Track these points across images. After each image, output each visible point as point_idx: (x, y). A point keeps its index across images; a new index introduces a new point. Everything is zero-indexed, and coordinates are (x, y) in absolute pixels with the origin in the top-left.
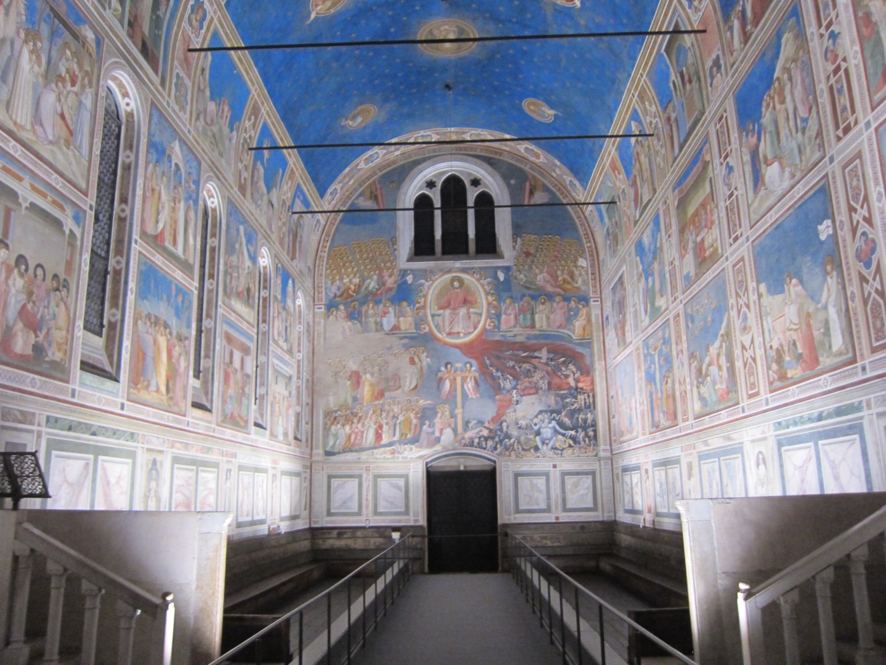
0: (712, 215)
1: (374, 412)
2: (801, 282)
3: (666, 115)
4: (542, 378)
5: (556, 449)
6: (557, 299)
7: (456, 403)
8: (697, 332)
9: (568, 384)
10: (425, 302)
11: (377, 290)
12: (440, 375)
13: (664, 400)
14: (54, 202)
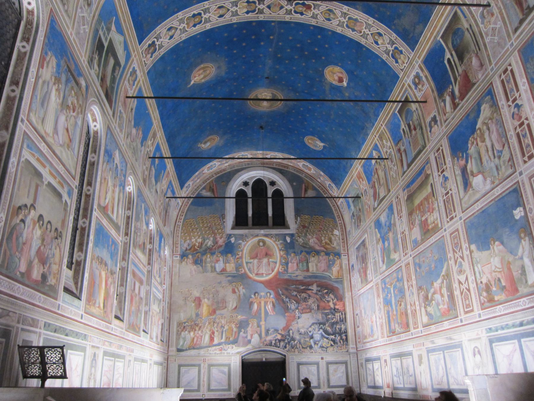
0: (433, 205)
1: (209, 323)
2: (502, 243)
3: (398, 148)
4: (313, 302)
5: (323, 347)
6: (322, 254)
7: (261, 318)
8: (423, 274)
9: (329, 306)
10: (242, 254)
11: (213, 246)
12: (251, 300)
13: (399, 316)
14: (59, 182)
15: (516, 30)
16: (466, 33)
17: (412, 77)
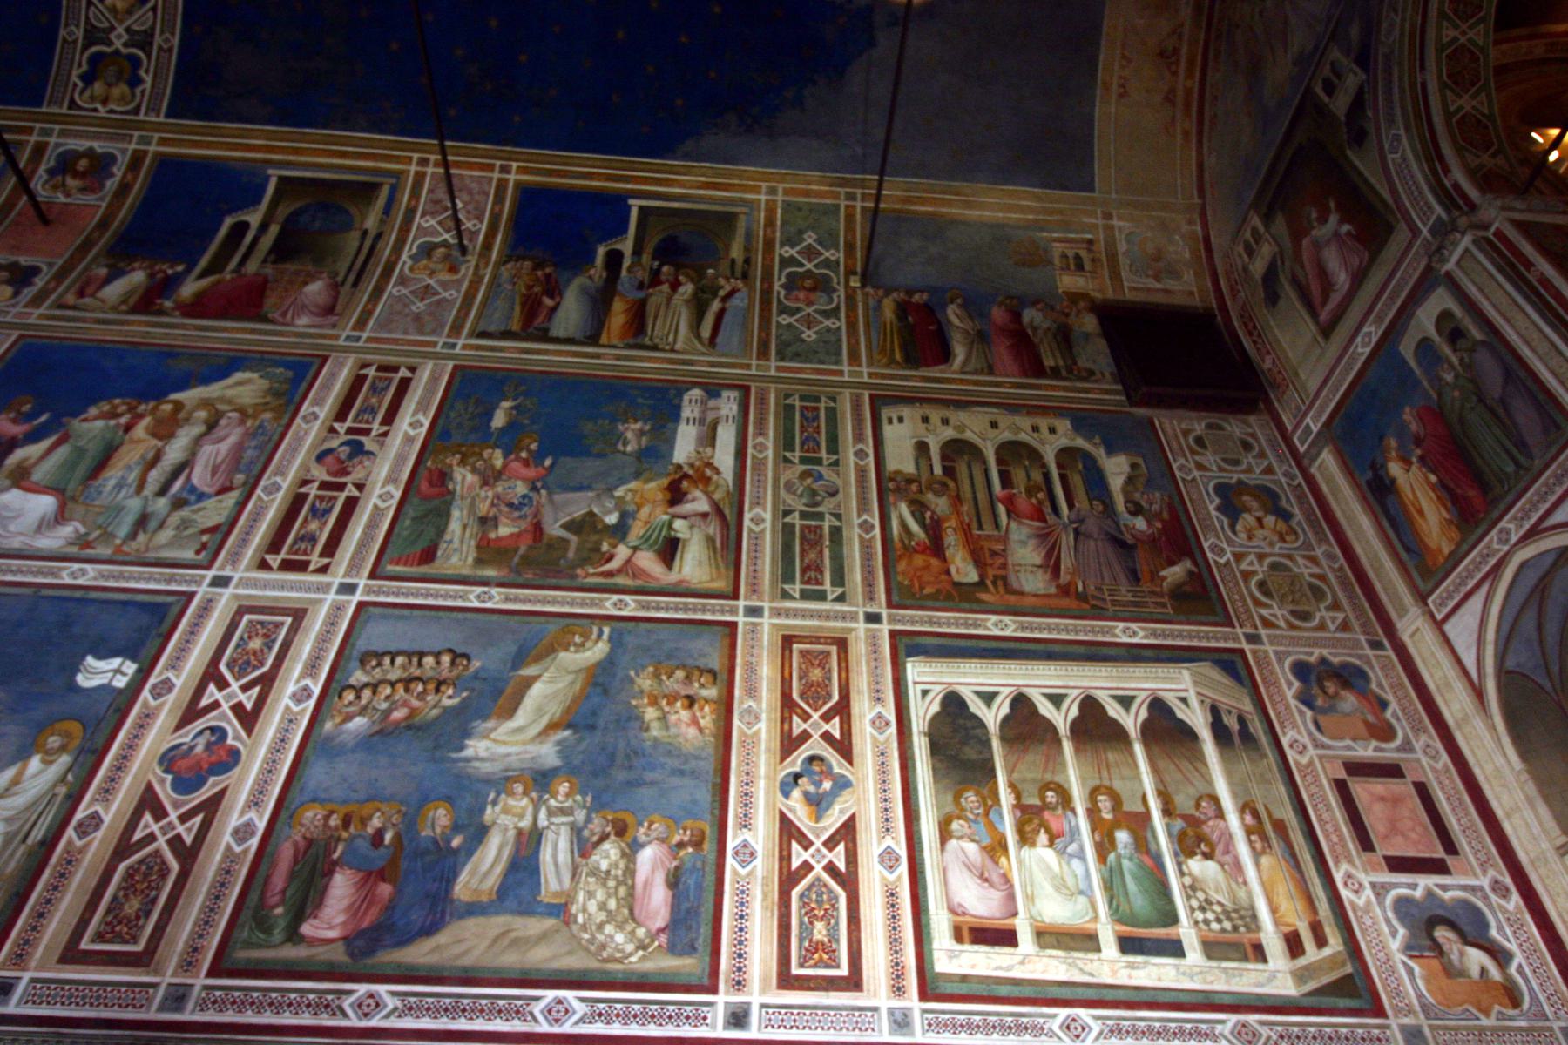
15: (483, 335)
17: (82, 144)
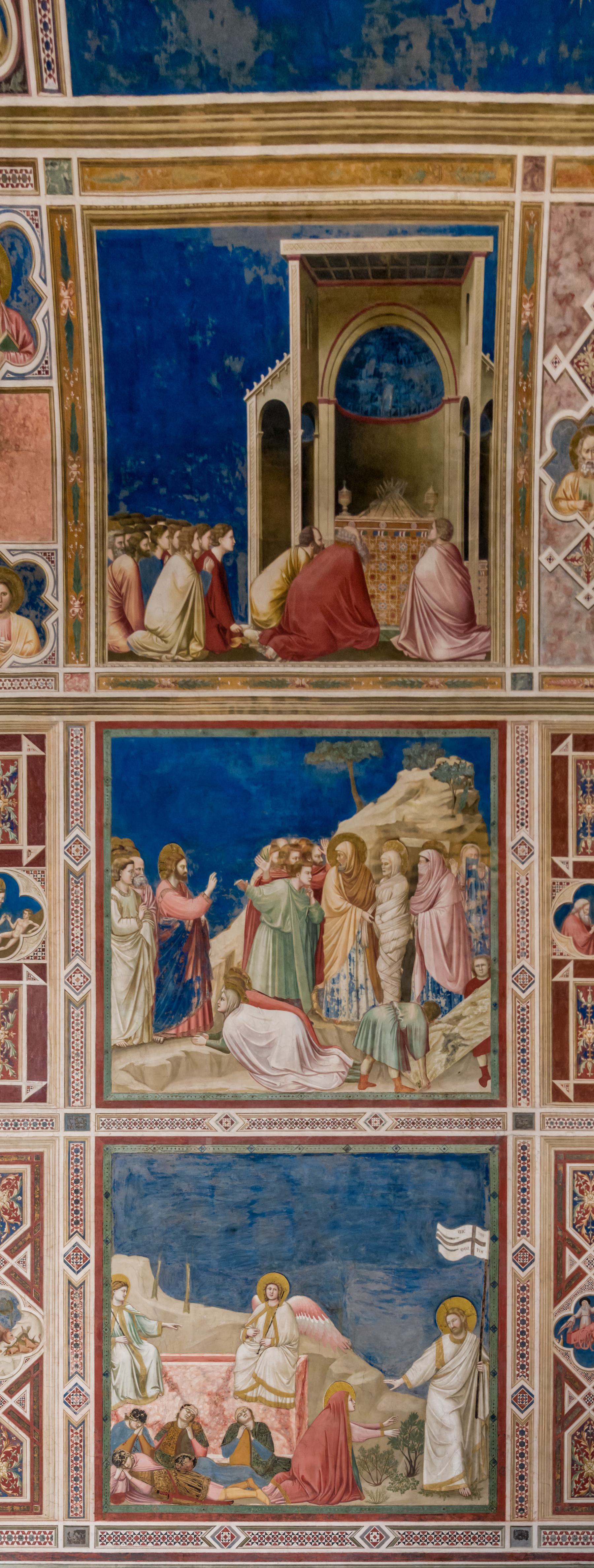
16: (450, 414)
